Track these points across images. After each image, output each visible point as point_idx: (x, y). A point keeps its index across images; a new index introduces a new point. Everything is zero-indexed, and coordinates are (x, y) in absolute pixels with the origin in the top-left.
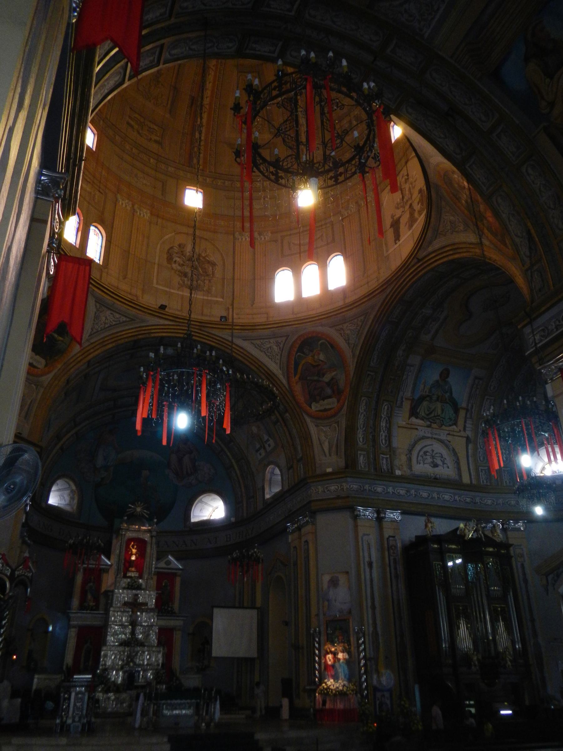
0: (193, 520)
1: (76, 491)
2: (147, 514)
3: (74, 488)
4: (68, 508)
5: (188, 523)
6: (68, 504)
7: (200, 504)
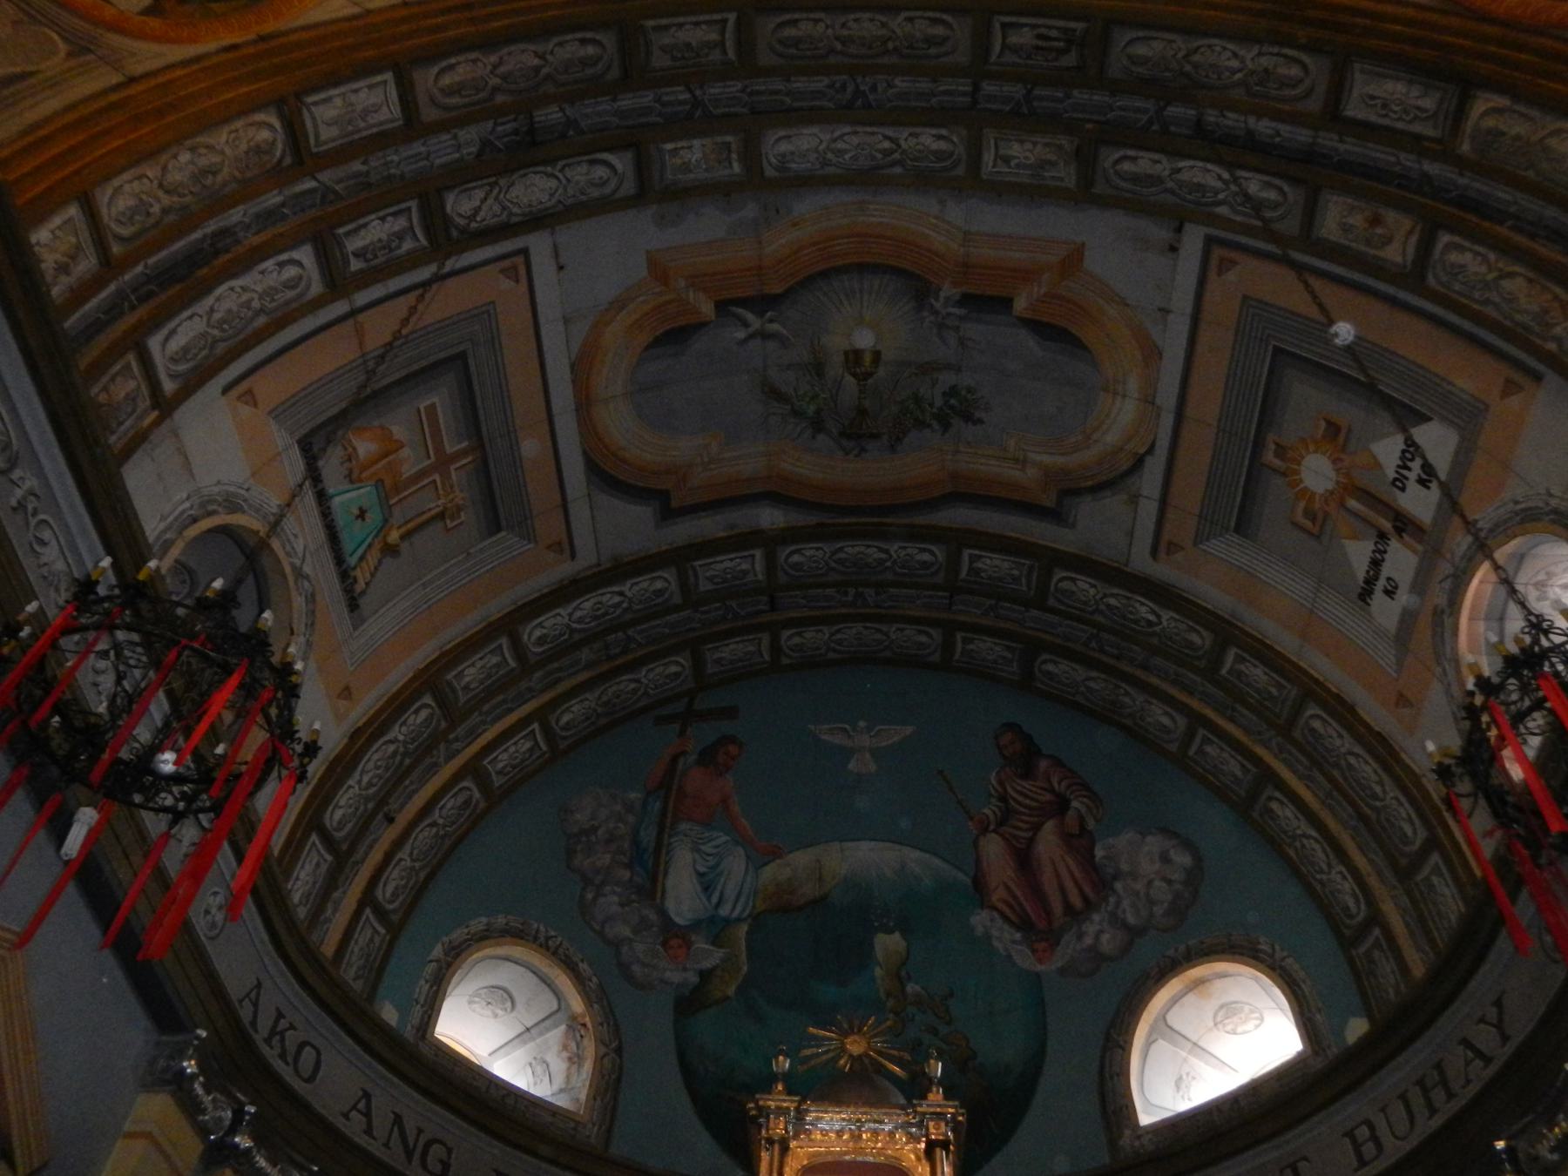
0: (1145, 1119)
1: (587, 1019)
2: (899, 1062)
3: (577, 1004)
4: (562, 1102)
5: (1127, 1132)
6: (561, 1091)
7: (1161, 1046)
